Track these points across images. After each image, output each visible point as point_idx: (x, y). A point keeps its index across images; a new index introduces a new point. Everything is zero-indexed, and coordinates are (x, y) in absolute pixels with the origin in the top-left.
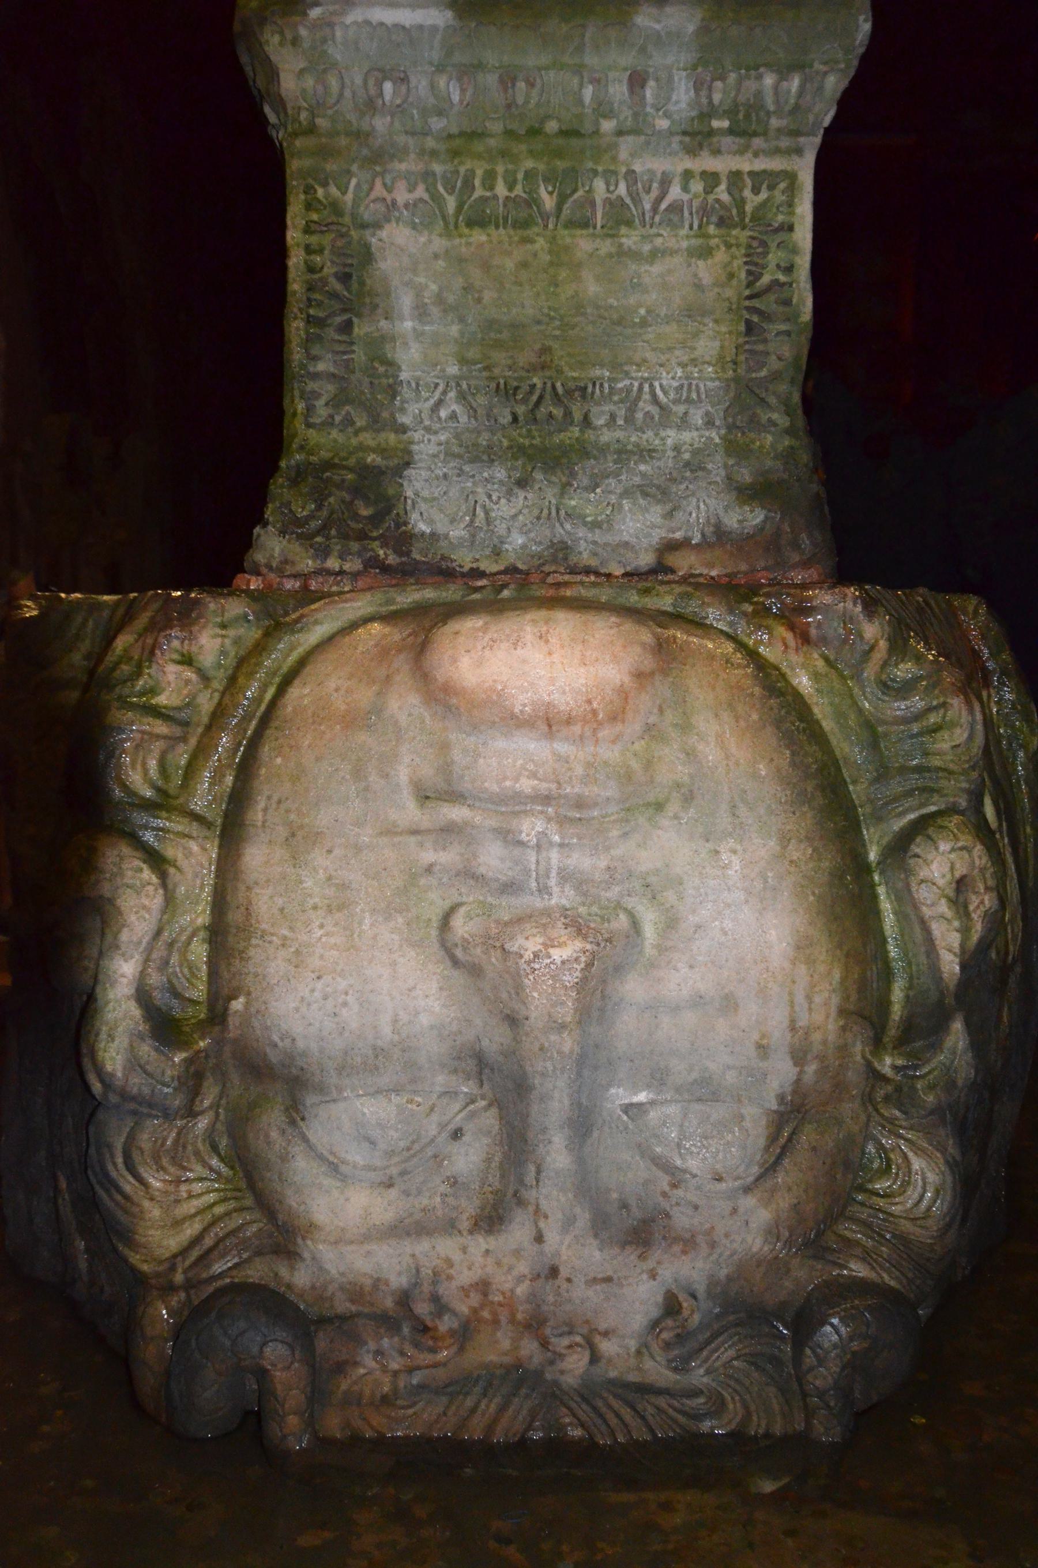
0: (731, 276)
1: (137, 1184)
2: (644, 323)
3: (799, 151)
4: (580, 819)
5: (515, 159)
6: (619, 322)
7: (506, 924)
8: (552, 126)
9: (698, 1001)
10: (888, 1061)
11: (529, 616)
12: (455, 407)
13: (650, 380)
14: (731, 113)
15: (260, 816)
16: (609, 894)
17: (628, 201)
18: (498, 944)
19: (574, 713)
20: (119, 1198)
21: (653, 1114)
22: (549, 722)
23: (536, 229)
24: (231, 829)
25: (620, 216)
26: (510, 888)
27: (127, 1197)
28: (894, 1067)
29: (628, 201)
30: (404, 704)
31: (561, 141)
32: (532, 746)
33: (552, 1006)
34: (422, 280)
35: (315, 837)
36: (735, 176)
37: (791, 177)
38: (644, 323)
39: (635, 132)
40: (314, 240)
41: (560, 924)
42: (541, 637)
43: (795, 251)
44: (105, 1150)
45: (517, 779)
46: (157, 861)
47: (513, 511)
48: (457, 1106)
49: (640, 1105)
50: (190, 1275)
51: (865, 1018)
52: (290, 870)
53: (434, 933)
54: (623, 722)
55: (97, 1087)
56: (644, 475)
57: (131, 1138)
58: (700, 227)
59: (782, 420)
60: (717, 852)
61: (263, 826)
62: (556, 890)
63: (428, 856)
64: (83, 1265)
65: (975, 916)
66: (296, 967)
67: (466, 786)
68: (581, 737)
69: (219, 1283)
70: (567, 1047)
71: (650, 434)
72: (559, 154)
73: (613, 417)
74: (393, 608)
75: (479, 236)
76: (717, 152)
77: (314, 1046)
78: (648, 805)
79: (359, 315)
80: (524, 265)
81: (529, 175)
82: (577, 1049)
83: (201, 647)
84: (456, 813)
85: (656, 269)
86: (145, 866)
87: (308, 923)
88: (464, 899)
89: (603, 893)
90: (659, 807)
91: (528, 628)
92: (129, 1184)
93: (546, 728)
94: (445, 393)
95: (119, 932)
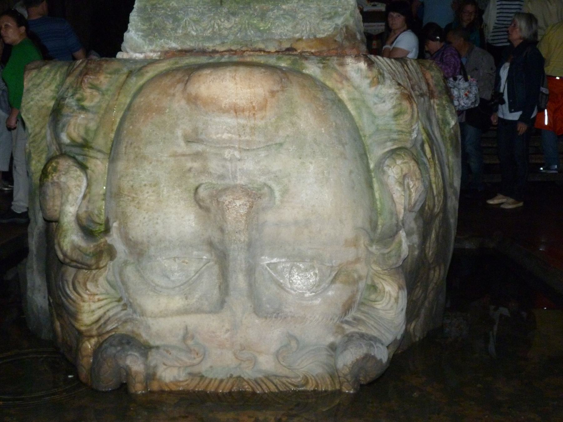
1: (77, 296)
4: (248, 150)
7: (220, 191)
9: (296, 223)
10: (374, 247)
11: (229, 69)
15: (124, 149)
16: (261, 180)
18: (216, 199)
19: (245, 107)
20: (71, 301)
21: (280, 267)
22: (236, 110)
24: (113, 156)
26: (222, 177)
27: (74, 301)
28: (377, 249)
30: (178, 104)
32: (229, 120)
33: (237, 222)
35: (144, 158)
41: (240, 191)
42: (233, 77)
44: (65, 282)
45: (223, 133)
46: (83, 167)
47: (230, 26)
48: (202, 265)
49: (274, 263)
50: (100, 330)
51: (365, 230)
52: (135, 171)
53: (192, 195)
54: (266, 111)
55: (61, 256)
56: (284, 10)
57: (75, 277)
60: (304, 163)
61: (125, 154)
62: (239, 177)
63: (189, 164)
64: (59, 329)
65: (412, 190)
66: (138, 208)
67: (203, 137)
68: (249, 117)
69: (110, 334)
70: (242, 240)
74: (177, 66)
77: (145, 240)
78: (276, 144)
82: (247, 240)
83: (101, 82)
84: (199, 148)
86: (78, 169)
87: (142, 192)
88: (204, 182)
89: (258, 179)
90: (281, 144)
91: (228, 74)
92: (74, 296)
93: (235, 114)
95: (68, 195)
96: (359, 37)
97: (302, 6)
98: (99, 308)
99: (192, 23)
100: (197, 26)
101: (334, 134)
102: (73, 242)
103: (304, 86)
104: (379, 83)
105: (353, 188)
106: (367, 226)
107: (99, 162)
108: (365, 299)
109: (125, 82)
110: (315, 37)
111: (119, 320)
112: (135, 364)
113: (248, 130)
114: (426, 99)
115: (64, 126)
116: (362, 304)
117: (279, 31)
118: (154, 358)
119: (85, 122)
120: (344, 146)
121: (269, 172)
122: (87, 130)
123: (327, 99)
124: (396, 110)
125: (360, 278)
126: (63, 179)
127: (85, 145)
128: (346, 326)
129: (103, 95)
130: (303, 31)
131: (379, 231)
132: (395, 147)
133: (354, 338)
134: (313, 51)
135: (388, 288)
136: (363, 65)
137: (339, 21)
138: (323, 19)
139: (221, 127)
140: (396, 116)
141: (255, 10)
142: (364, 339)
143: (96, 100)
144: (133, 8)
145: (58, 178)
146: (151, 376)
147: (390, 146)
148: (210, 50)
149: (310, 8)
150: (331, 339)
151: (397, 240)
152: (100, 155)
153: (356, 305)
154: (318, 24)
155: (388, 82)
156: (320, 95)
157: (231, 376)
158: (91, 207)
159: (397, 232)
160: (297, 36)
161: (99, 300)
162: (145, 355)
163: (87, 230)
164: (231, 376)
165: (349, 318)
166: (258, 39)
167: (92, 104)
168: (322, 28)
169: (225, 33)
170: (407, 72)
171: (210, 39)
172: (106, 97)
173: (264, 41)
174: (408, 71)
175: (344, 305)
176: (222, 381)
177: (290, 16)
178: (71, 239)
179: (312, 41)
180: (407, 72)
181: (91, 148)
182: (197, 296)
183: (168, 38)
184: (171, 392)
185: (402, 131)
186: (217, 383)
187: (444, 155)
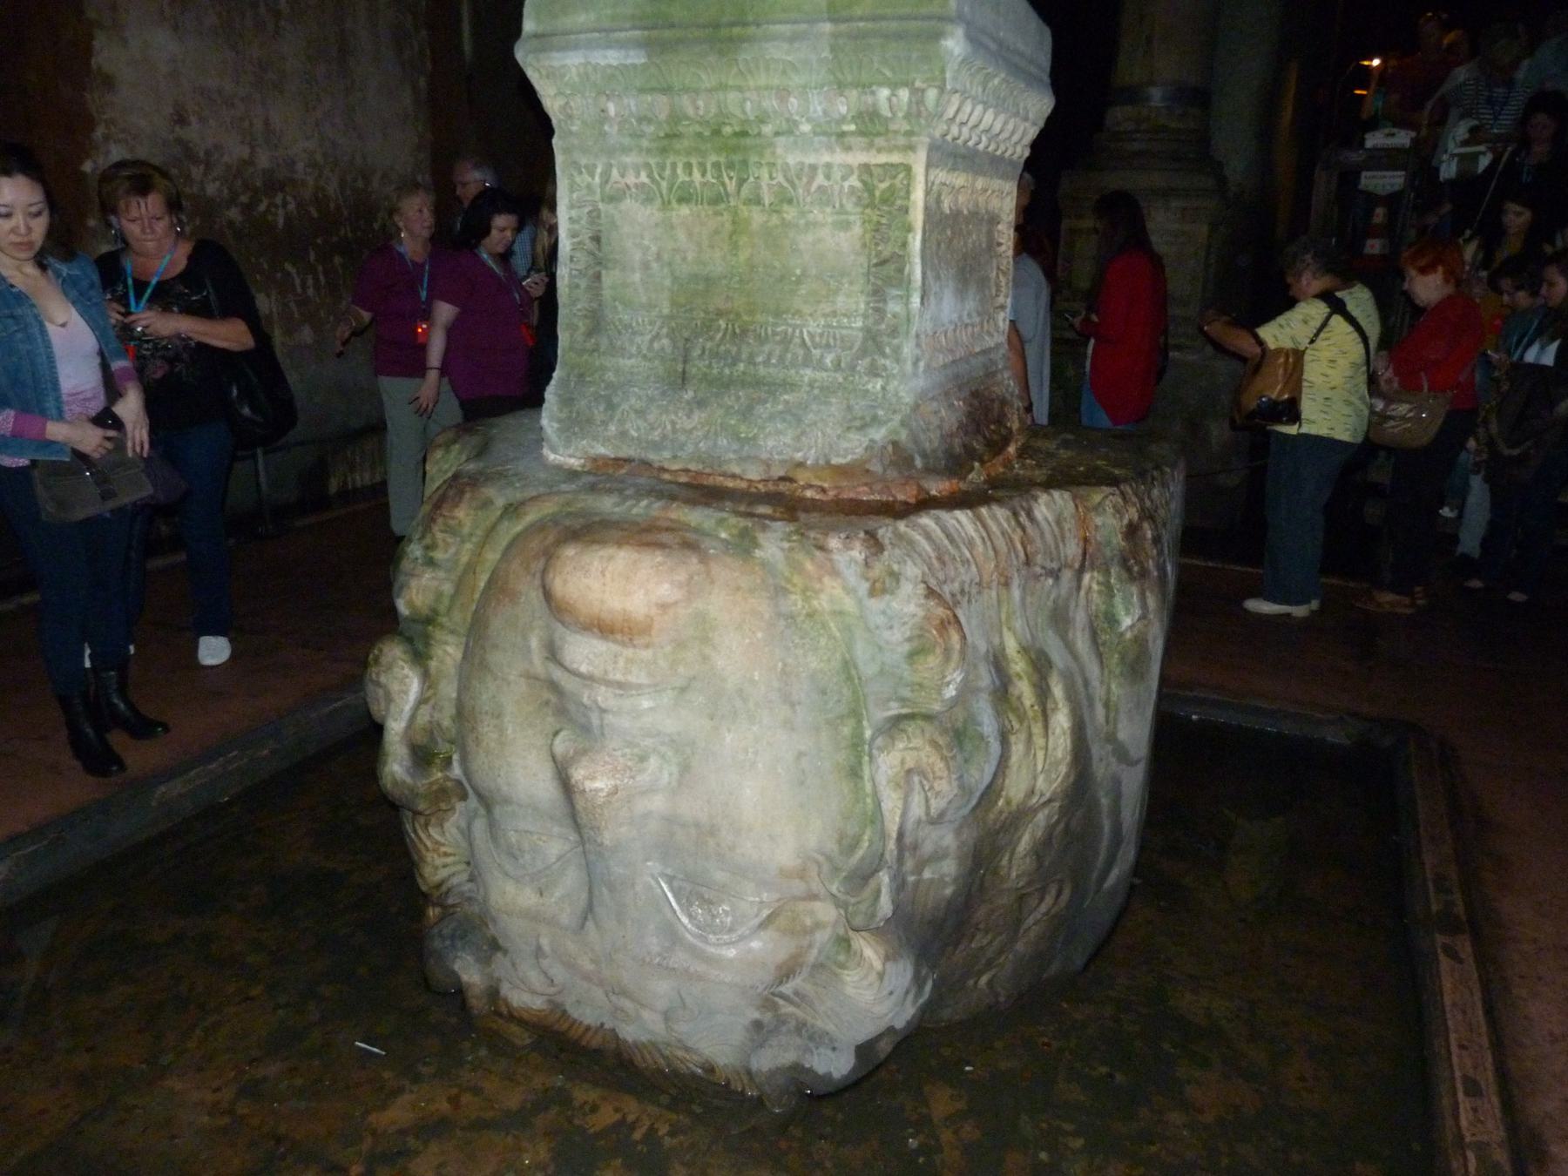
0: (864, 245)
2: (799, 282)
3: (911, 148)
5: (703, 154)
6: (782, 278)
8: (727, 130)
11: (601, 553)
12: (665, 341)
13: (801, 327)
14: (859, 117)
17: (786, 184)
23: (723, 206)
29: (786, 184)
31: (734, 141)
34: (646, 242)
36: (866, 168)
37: (908, 169)
39: (790, 132)
40: (574, 213)
46: (419, 658)
56: (787, 402)
58: (842, 206)
71: (793, 372)
72: (735, 149)
73: (770, 356)
75: (685, 210)
76: (848, 149)
79: (606, 268)
80: (716, 232)
81: (716, 165)
85: (810, 238)
94: (661, 328)
96: (919, 463)
97: (816, 398)
98: (445, 866)
99: (633, 415)
100: (640, 422)
101: (776, 684)
102: (393, 774)
103: (738, 589)
104: (884, 591)
105: (802, 783)
106: (832, 846)
107: (450, 649)
108: (828, 958)
109: (493, 527)
110: (828, 462)
111: (462, 893)
112: (470, 972)
113: (621, 663)
114: (1067, 575)
115: (401, 588)
116: (818, 967)
117: (771, 443)
118: (500, 964)
119: (436, 583)
120: (793, 705)
121: (659, 734)
122: (439, 595)
123: (779, 615)
124: (915, 643)
125: (818, 925)
126: (383, 679)
127: (430, 620)
128: (781, 1002)
129: (463, 542)
130: (810, 448)
131: (860, 853)
132: (904, 711)
133: (784, 1029)
134: (826, 485)
135: (869, 952)
136: (858, 553)
137: (879, 434)
138: (849, 428)
139: (584, 652)
140: (912, 656)
141: (738, 398)
142: (800, 1035)
143: (452, 550)
144: (550, 378)
145: (378, 674)
146: (493, 994)
147: (895, 709)
148: (656, 465)
149: (829, 404)
150: (756, 1015)
151: (872, 883)
152: (450, 638)
153: (806, 971)
154: (839, 437)
155: (907, 588)
156: (764, 607)
157: (602, 1025)
158: (437, 716)
159: (876, 871)
160: (799, 456)
161: (446, 854)
162: (485, 960)
163: (423, 756)
164: (602, 1025)
165: (787, 989)
166: (732, 456)
167: (447, 556)
168: (845, 445)
169: (683, 438)
170: (1024, 529)
171: (657, 446)
172: (468, 546)
173: (742, 460)
174: (1027, 524)
175: (779, 968)
176: (588, 1028)
177: (794, 415)
178: (396, 766)
179: (823, 468)
180: (1024, 529)
181: (442, 626)
182: (557, 894)
183: (595, 438)
184: (521, 1022)
185: (920, 685)
186: (582, 1029)
187: (1095, 683)
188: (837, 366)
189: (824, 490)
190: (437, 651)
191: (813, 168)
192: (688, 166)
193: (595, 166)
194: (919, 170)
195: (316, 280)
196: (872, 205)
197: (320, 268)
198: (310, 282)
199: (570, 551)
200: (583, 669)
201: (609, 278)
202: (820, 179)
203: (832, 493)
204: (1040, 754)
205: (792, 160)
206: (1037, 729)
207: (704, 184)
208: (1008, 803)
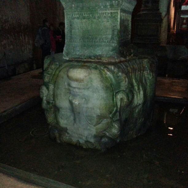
2: (102, 30)
3: (118, 10)
23: (90, 19)
25: (99, 17)
36: (111, 13)
37: (117, 13)
38: (102, 30)
43: (118, 21)
46: (48, 88)
59: (115, 42)
75: (84, 20)
85: (103, 23)
113: (79, 85)
139: (74, 84)
152: (52, 85)
178: (44, 105)
188: (108, 42)
189: (106, 60)
190: (50, 87)
191: (103, 13)
192: (85, 14)
193: (70, 14)
194: (119, 13)
195: (13, 37)
196: (112, 18)
197: (13, 36)
198: (12, 38)
199: (71, 70)
200: (74, 86)
201: (73, 31)
202: (104, 15)
203: (107, 61)
204: (139, 98)
205: (100, 12)
206: (138, 94)
207: (87, 16)
208: (135, 104)
